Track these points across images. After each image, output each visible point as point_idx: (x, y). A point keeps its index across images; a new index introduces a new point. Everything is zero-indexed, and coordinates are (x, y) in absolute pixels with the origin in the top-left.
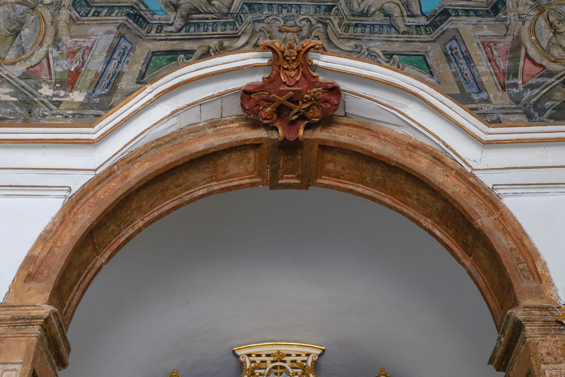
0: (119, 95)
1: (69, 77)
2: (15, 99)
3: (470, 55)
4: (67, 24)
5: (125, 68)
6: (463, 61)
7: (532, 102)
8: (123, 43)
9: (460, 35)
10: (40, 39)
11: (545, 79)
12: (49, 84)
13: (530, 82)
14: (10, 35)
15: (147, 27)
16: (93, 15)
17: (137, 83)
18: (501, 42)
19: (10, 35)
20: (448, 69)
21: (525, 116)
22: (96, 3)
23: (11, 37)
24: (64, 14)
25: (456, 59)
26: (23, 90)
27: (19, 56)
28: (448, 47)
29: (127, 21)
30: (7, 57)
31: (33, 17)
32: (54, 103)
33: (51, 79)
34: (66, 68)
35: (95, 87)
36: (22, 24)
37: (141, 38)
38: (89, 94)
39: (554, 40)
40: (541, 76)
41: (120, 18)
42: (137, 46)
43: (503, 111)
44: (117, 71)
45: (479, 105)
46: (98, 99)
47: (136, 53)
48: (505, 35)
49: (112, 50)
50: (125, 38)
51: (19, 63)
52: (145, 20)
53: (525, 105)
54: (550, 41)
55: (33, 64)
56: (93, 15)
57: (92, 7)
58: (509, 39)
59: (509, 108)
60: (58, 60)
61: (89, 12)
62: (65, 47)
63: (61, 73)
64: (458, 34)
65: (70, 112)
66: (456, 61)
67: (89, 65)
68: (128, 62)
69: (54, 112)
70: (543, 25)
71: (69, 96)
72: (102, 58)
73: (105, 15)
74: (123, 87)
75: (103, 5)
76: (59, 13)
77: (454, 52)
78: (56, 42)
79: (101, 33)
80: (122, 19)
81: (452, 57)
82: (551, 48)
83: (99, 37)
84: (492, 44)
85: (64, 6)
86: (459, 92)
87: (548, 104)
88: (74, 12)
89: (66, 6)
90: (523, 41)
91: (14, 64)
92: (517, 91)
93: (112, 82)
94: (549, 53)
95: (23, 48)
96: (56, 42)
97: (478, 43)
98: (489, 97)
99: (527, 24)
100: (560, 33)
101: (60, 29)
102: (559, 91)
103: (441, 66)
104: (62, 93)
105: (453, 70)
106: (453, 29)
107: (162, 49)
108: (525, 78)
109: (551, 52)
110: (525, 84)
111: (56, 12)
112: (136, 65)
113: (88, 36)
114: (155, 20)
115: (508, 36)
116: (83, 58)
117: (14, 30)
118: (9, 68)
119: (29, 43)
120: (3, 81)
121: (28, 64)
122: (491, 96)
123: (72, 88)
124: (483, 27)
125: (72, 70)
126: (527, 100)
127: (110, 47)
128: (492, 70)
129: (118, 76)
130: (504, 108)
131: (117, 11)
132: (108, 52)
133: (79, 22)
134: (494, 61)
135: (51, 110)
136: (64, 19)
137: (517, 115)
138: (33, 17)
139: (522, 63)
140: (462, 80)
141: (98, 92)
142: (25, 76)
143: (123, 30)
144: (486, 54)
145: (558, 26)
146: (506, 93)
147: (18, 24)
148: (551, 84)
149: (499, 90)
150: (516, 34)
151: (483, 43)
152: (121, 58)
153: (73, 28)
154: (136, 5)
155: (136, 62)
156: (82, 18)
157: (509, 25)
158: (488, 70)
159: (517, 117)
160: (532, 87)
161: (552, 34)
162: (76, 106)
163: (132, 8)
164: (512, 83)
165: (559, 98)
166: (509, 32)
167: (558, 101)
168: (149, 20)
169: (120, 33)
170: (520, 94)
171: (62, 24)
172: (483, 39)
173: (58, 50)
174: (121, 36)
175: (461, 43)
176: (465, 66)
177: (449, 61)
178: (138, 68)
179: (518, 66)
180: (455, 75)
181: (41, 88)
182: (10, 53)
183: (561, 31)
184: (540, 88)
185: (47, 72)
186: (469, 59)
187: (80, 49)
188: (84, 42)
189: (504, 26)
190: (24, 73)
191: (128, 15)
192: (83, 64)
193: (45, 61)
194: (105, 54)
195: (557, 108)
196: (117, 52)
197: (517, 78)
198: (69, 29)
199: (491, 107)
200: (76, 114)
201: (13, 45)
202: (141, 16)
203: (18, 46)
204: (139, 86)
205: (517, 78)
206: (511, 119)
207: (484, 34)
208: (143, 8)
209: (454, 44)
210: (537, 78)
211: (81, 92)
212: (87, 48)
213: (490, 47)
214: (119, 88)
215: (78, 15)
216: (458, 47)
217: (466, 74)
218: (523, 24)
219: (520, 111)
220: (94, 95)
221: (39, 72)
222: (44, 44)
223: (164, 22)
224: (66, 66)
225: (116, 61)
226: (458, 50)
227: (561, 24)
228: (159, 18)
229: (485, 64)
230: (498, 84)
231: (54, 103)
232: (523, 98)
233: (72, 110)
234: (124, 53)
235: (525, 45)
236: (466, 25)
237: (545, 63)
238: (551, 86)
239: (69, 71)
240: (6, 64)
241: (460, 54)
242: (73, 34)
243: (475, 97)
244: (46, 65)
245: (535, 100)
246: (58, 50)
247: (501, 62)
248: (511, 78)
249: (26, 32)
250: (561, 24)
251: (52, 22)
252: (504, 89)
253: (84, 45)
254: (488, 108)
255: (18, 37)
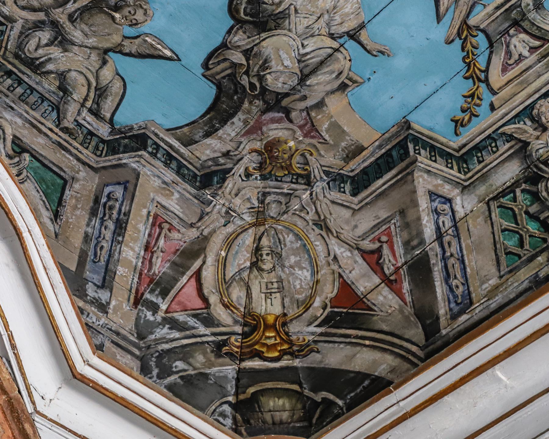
3: (127, 223)
6: (111, 225)
7: (160, 348)
9: (136, 185)
11: (198, 324)
13: (175, 315)
18: (179, 231)
20: (84, 222)
21: (139, 363)
25: (104, 215)
28: (107, 190)
39: (245, 274)
40: (195, 316)
43: (115, 338)
45: (88, 308)
48: (192, 225)
53: (149, 347)
54: (241, 271)
58: (193, 234)
59: (125, 338)
64: (134, 181)
66: (102, 219)
70: (247, 242)
77: (110, 203)
81: (101, 209)
82: (235, 283)
84: (166, 226)
86: (73, 268)
87: (180, 365)
90: (208, 249)
92: (152, 319)
94: (227, 289)
97: (149, 212)
98: (108, 303)
99: (230, 228)
100: (260, 270)
102: (205, 354)
103: (78, 212)
105: (90, 230)
106: (134, 170)
108: (174, 306)
109: (230, 290)
110: (167, 315)
115: (195, 229)
122: (113, 303)
124: (173, 193)
126: (156, 340)
128: (140, 264)
130: (118, 334)
134: (152, 253)
137: (129, 356)
139: (184, 279)
140: (91, 253)
144: (150, 235)
145: (265, 257)
146: (136, 311)
148: (200, 336)
149: (129, 300)
150: (205, 233)
151: (156, 216)
157: (207, 214)
158: (134, 261)
159: (126, 359)
160: (174, 325)
161: (248, 264)
164: (152, 302)
165: (198, 365)
166: (199, 224)
167: (195, 369)
170: (151, 326)
172: (161, 212)
175: (128, 195)
176: (108, 235)
177: (93, 213)
179: (176, 280)
180: (87, 238)
183: (264, 267)
184: (183, 334)
186: (121, 228)
189: (199, 211)
195: (187, 380)
197: (164, 299)
199: (103, 321)
205: (164, 299)
206: (118, 357)
207: (167, 205)
209: (119, 192)
210: (188, 315)
213: (161, 228)
216: (120, 199)
217: (102, 247)
218: (225, 226)
219: (137, 352)
226: (117, 205)
227: (269, 258)
229: (137, 249)
230: (133, 291)
232: (152, 333)
235: (205, 257)
236: (154, 176)
237: (213, 299)
238: (198, 340)
241: (115, 212)
243: (91, 291)
245: (166, 346)
247: (160, 260)
248: (157, 292)
250: (269, 258)
252: (136, 303)
254: (98, 319)
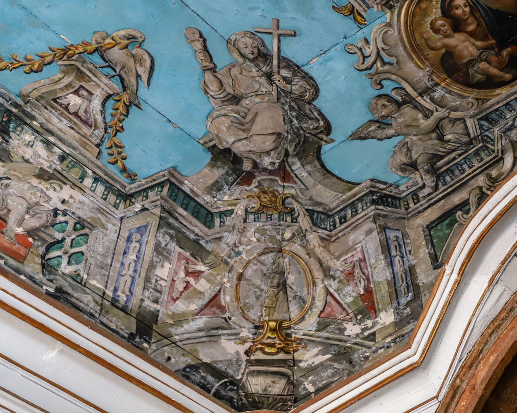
0: (426, 292)
1: (364, 302)
2: (329, 356)
4: (324, 247)
5: (412, 260)
8: (391, 235)
10: (310, 278)
12: (350, 320)
14: (279, 292)
15: (402, 203)
16: (341, 223)
17: (435, 268)
19: (279, 292)
22: (334, 209)
23: (281, 293)
24: (313, 239)
26: (330, 341)
27: (303, 308)
29: (377, 209)
30: (292, 316)
31: (287, 260)
32: (366, 338)
33: (348, 314)
34: (355, 294)
35: (397, 298)
36: (282, 273)
37: (404, 218)
38: (396, 309)
41: (369, 210)
42: (407, 230)
44: (406, 267)
46: (408, 309)
47: (411, 238)
49: (386, 248)
50: (389, 228)
51: (307, 316)
52: (394, 198)
55: (321, 308)
56: (341, 223)
57: (333, 215)
60: (341, 290)
61: (334, 221)
62: (339, 272)
63: (354, 302)
65: (389, 339)
67: (374, 277)
68: (410, 251)
69: (374, 348)
71: (377, 322)
72: (382, 263)
73: (353, 216)
74: (424, 281)
75: (341, 207)
76: (307, 241)
78: (326, 271)
79: (362, 237)
80: (371, 210)
83: (364, 242)
85: (306, 230)
88: (320, 231)
89: (309, 230)
91: (303, 319)
93: (410, 283)
95: (300, 297)
96: (326, 271)
101: (320, 256)
104: (369, 323)
107: (434, 217)
111: (304, 241)
112: (421, 250)
113: (352, 247)
114: (404, 191)
116: (363, 273)
117: (278, 286)
118: (301, 326)
119: (302, 289)
120: (305, 344)
121: (316, 311)
123: (375, 312)
125: (362, 292)
127: (382, 246)
129: (411, 271)
131: (360, 205)
132: (383, 253)
133: (333, 239)
135: (369, 348)
136: (316, 244)
138: (287, 260)
141: (403, 301)
142: (322, 326)
143: (381, 221)
147: (277, 276)
152: (400, 252)
153: (332, 247)
154: (373, 187)
155: (419, 248)
156: (333, 232)
162: (391, 330)
163: (372, 193)
168: (398, 196)
169: (380, 225)
171: (319, 251)
173: (334, 280)
174: (383, 229)
178: (424, 252)
181: (345, 329)
182: (291, 309)
185: (340, 309)
187: (354, 266)
188: (353, 256)
190: (319, 323)
191: (373, 202)
192: (368, 279)
193: (329, 298)
194: (382, 257)
196: (392, 247)
198: (329, 251)
200: (396, 339)
201: (289, 299)
202: (387, 196)
203: (295, 297)
204: (439, 270)
208: (382, 186)
211: (387, 312)
212: (360, 261)
214: (421, 284)
215: (327, 232)
220: (401, 307)
221: (333, 314)
222: (317, 281)
223: (414, 188)
224: (353, 291)
225: (398, 258)
228: (407, 187)
231: (366, 338)
233: (390, 335)
234: (400, 245)
239: (361, 295)
240: (296, 324)
242: (337, 254)
244: (333, 302)
246: (334, 280)
249: (291, 279)
251: (308, 254)
253: (355, 259)
255: (289, 289)
